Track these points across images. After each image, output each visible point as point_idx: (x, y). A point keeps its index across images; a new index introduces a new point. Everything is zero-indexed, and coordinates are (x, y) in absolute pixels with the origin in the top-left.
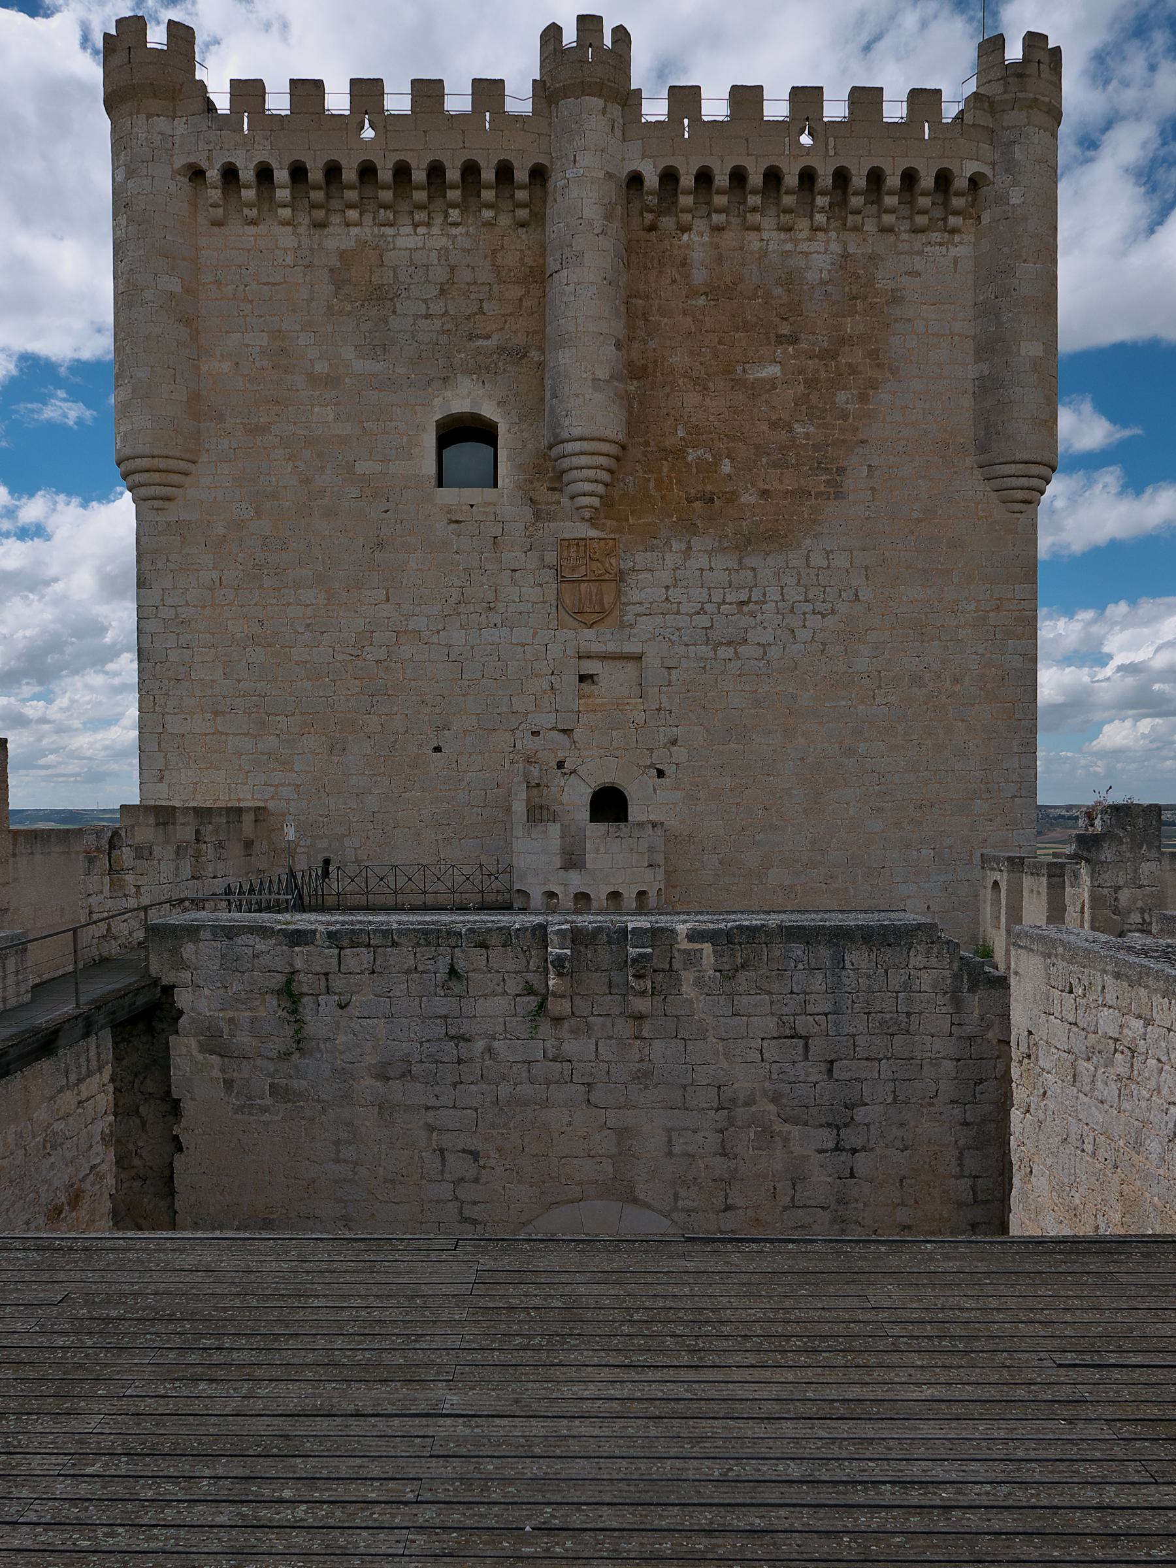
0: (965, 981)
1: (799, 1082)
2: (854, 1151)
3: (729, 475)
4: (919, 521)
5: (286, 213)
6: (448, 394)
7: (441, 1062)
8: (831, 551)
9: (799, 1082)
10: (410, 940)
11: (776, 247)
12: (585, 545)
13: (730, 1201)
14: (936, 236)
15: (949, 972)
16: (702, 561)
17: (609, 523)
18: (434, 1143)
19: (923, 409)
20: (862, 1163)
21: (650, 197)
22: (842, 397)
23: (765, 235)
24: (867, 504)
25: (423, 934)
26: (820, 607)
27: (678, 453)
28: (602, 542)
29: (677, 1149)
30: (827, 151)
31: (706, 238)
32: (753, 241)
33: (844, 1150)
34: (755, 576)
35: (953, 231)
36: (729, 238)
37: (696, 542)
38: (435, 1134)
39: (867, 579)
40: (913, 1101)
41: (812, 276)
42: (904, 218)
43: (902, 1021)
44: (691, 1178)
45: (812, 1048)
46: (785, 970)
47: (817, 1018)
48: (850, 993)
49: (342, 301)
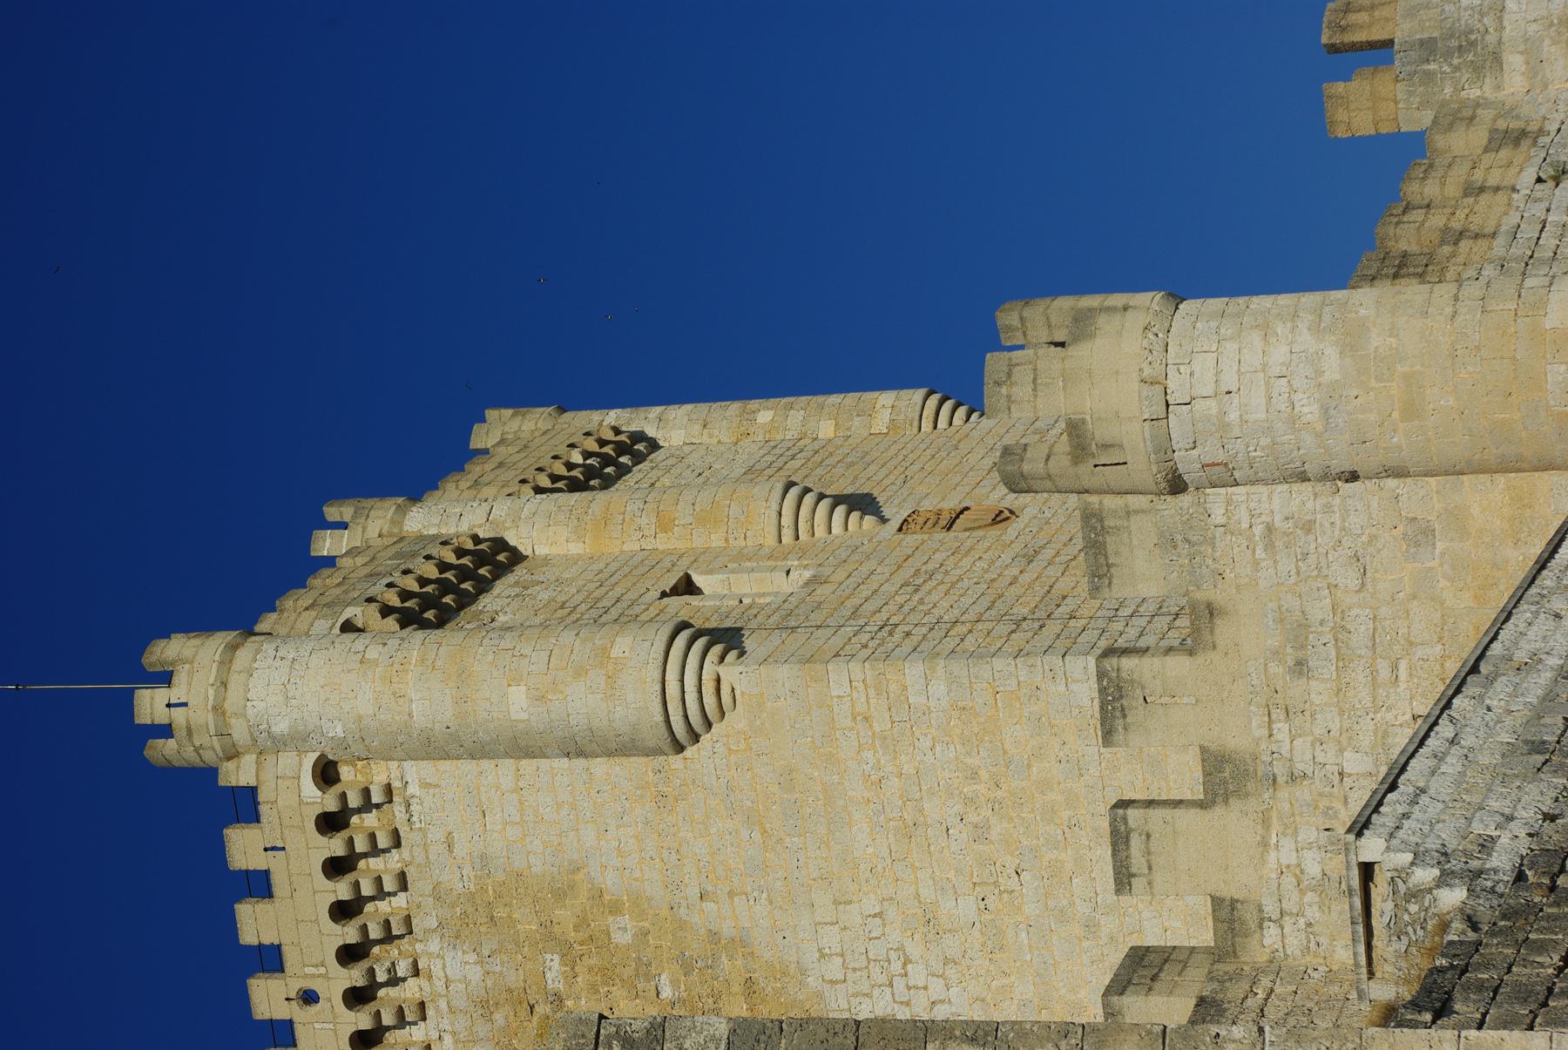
8: (820, 950)
11: (445, 1021)
19: (618, 827)
22: (622, 938)
26: (896, 967)
30: (320, 976)
39: (850, 902)
41: (475, 973)
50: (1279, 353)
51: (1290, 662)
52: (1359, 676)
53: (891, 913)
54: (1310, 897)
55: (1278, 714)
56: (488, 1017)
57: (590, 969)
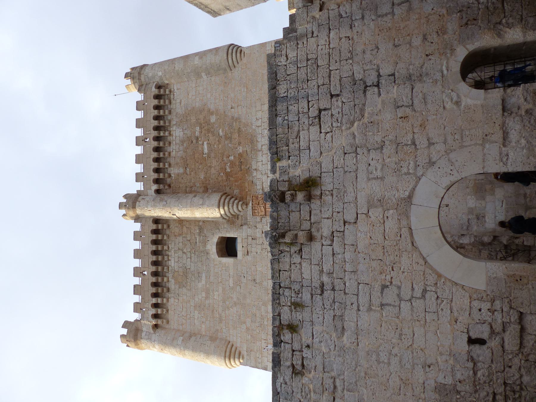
0: (292, 35)
1: (342, 111)
2: (379, 76)
3: (234, 157)
4: (247, 89)
5: (165, 300)
6: (211, 253)
7: (334, 299)
8: (256, 118)
9: (342, 111)
10: (277, 307)
11: (174, 147)
12: (254, 207)
13: (409, 143)
14: (172, 96)
15: (288, 44)
16: (260, 164)
17: (248, 198)
18: (378, 309)
20: (386, 70)
21: (161, 187)
23: (171, 150)
24: (242, 107)
25: (274, 301)
27: (228, 175)
28: (254, 201)
29: (379, 174)
30: (149, 133)
31: (172, 169)
32: (173, 154)
33: (378, 82)
34: (264, 145)
35: (170, 91)
36: (172, 161)
37: (254, 167)
38: (373, 308)
40: (351, 49)
42: (167, 107)
43: (311, 63)
44: (396, 166)
45: (325, 106)
46: (288, 125)
47: (310, 106)
48: (298, 91)
49: (187, 285)
56: (183, 145)
57: (205, 130)
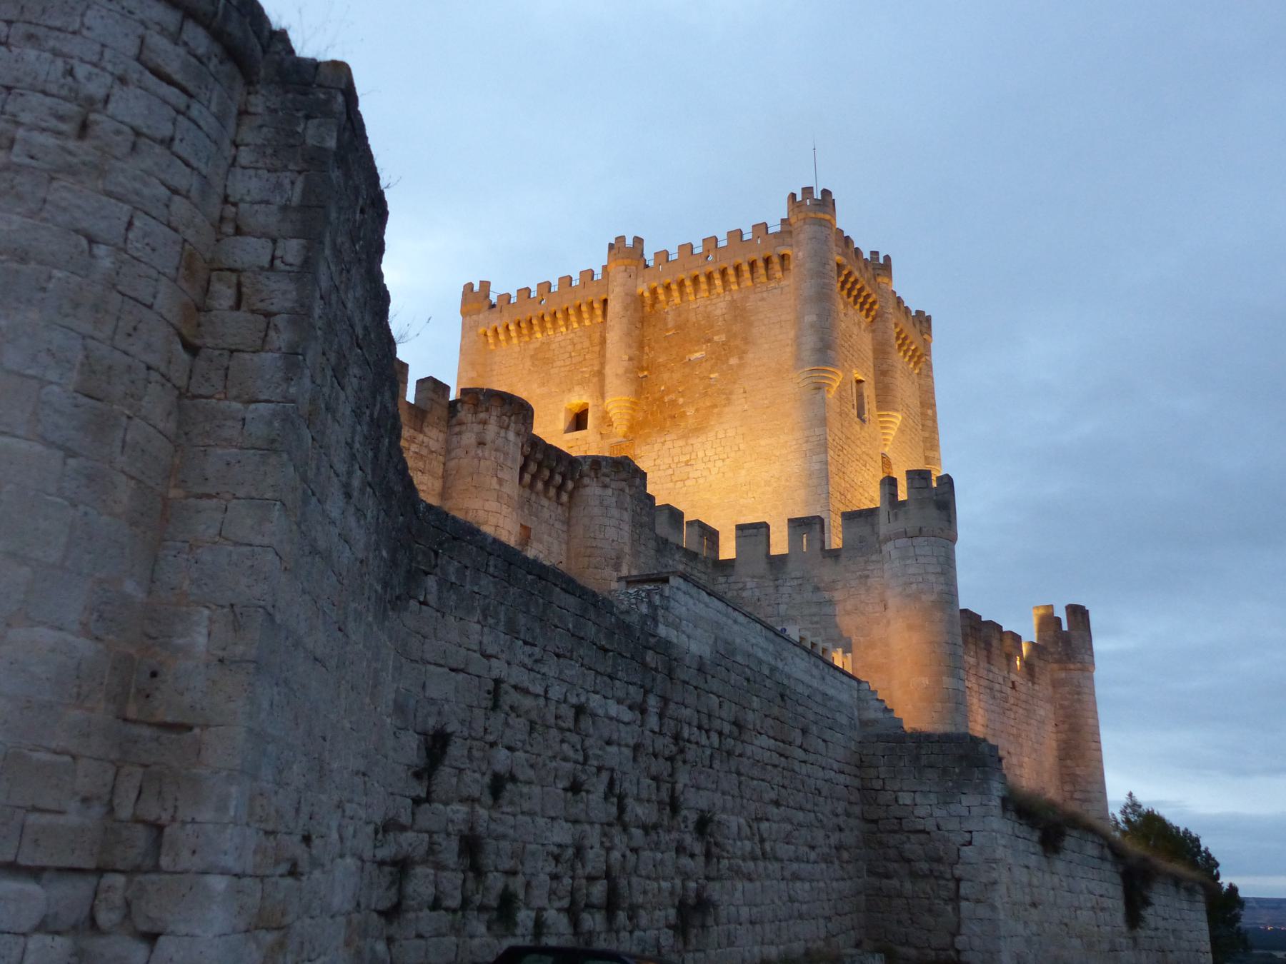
4: (768, 407)
37: (668, 438)
41: (718, 312)
50: (932, 578)
51: (819, 585)
52: (814, 610)
53: (740, 453)
54: (735, 593)
55: (800, 581)
